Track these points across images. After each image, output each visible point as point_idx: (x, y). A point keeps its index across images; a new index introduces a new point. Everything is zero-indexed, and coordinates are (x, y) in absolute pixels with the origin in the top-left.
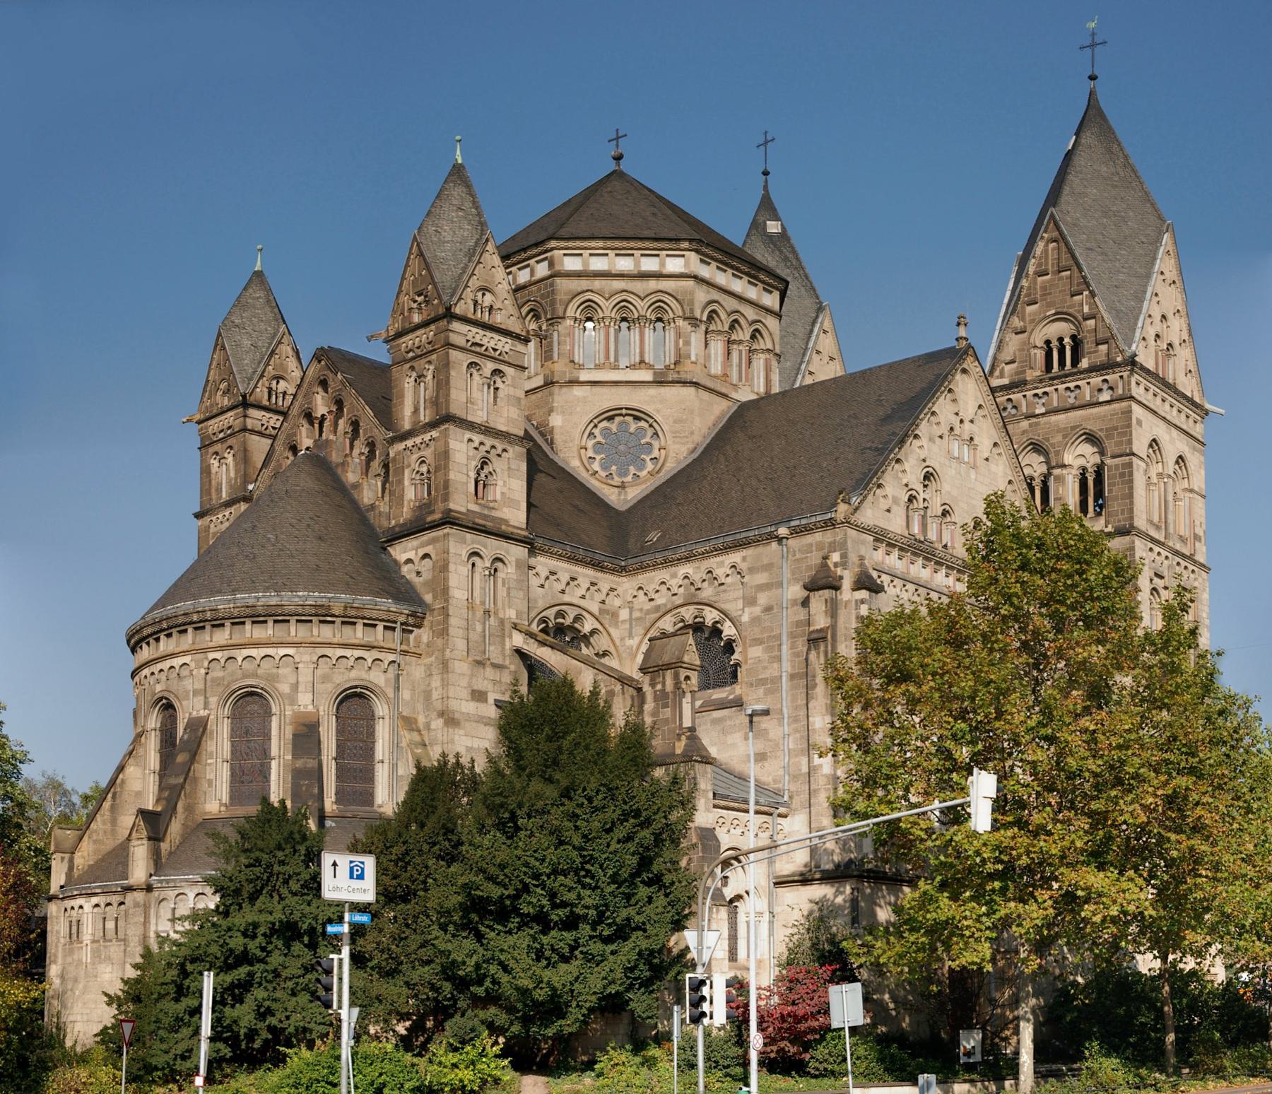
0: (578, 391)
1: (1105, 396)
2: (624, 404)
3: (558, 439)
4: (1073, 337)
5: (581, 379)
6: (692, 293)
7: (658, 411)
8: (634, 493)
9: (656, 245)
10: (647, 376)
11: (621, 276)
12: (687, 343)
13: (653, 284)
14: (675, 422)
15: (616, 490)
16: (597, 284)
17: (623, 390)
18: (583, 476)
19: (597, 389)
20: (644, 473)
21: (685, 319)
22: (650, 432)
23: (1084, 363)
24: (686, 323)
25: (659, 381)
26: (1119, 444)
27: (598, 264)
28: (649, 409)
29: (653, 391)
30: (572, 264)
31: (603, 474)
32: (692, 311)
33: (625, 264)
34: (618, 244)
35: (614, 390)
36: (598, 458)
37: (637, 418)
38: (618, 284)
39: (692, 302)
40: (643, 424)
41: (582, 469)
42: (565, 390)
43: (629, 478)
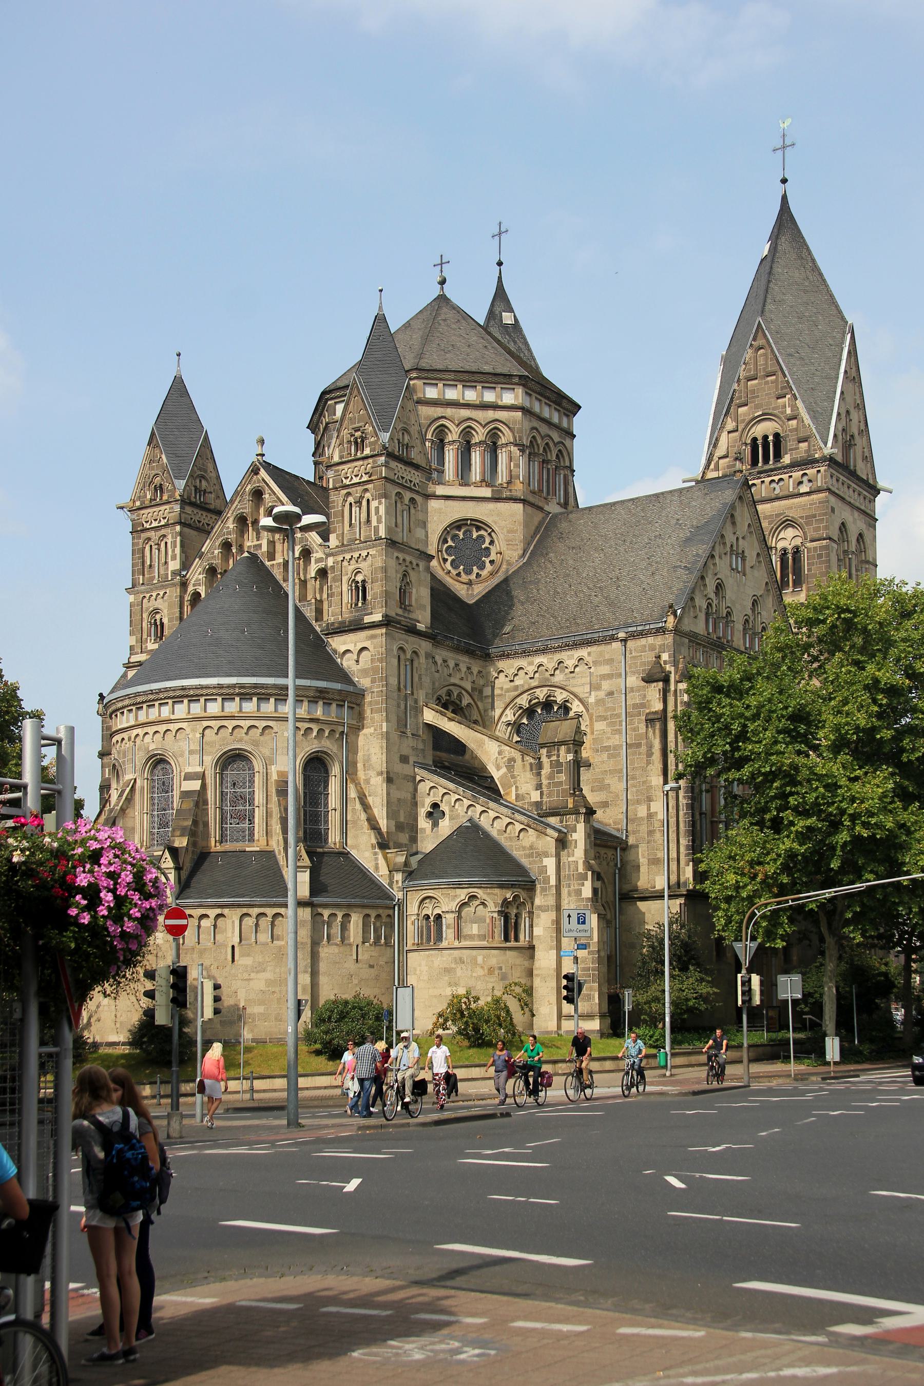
2: (470, 514)
4: (777, 436)
5: (437, 493)
7: (495, 523)
8: (479, 590)
10: (487, 492)
11: (467, 406)
12: (517, 466)
13: (491, 414)
14: (508, 532)
15: (465, 586)
16: (449, 412)
19: (450, 503)
20: (484, 573)
21: (516, 445)
22: (488, 540)
24: (516, 448)
25: (496, 499)
28: (489, 520)
29: (491, 506)
31: (454, 572)
35: (462, 503)
36: (450, 559)
37: (478, 528)
38: (465, 413)
40: (482, 532)
41: (439, 568)
43: (473, 577)
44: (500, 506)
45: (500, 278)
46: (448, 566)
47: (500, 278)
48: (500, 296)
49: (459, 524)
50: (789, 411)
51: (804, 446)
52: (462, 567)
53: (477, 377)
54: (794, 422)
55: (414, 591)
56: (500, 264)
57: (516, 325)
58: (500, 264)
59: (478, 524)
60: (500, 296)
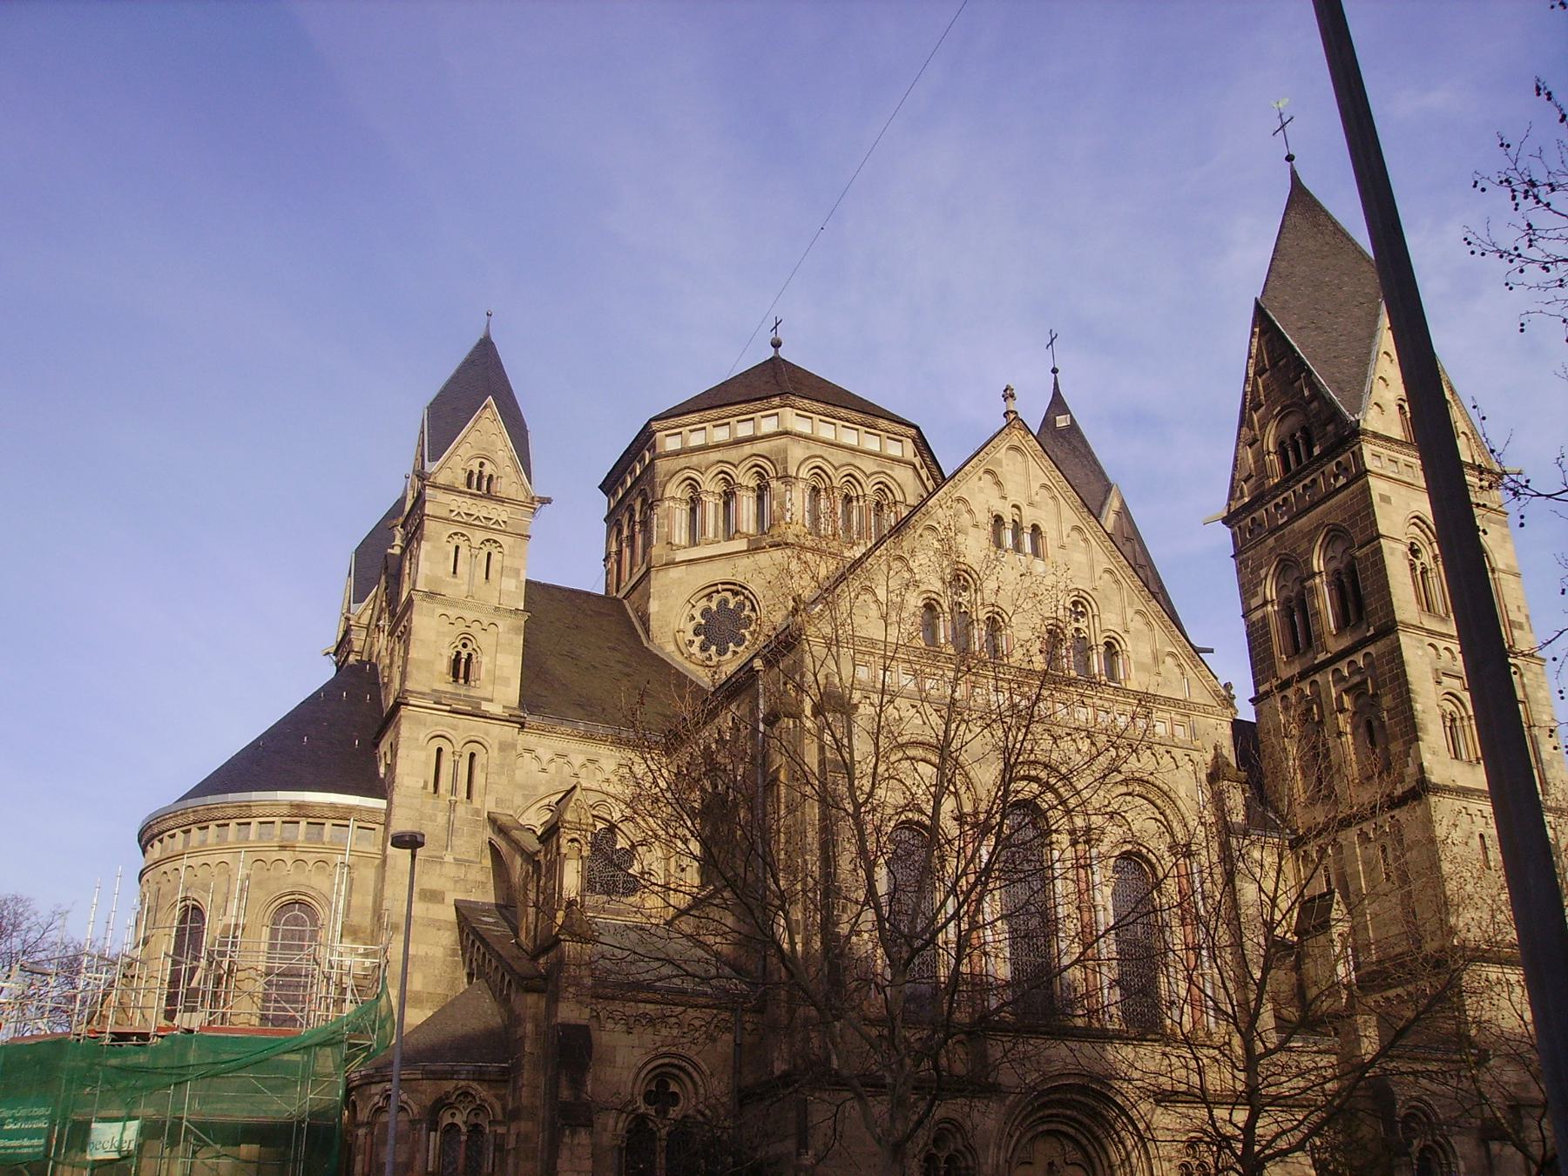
0: (674, 573)
1: (1342, 480)
3: (653, 624)
4: (1304, 430)
6: (785, 451)
9: (751, 406)
11: (717, 446)
13: (748, 449)
16: (695, 459)
17: (718, 564)
18: (678, 661)
21: (778, 479)
23: (1316, 451)
25: (754, 548)
27: (696, 439)
29: (745, 562)
30: (672, 444)
31: (701, 656)
32: (785, 469)
33: (721, 435)
34: (714, 413)
35: (708, 566)
36: (698, 640)
38: (714, 456)
39: (785, 461)
42: (661, 573)
44: (762, 558)
45: (1056, 384)
46: (695, 649)
47: (1056, 384)
48: (1058, 403)
49: (710, 591)
50: (1306, 393)
51: (1330, 428)
52: (714, 648)
53: (934, 469)
54: (1315, 404)
55: (485, 660)
56: (1055, 371)
57: (1073, 427)
59: (737, 589)
60: (1058, 403)
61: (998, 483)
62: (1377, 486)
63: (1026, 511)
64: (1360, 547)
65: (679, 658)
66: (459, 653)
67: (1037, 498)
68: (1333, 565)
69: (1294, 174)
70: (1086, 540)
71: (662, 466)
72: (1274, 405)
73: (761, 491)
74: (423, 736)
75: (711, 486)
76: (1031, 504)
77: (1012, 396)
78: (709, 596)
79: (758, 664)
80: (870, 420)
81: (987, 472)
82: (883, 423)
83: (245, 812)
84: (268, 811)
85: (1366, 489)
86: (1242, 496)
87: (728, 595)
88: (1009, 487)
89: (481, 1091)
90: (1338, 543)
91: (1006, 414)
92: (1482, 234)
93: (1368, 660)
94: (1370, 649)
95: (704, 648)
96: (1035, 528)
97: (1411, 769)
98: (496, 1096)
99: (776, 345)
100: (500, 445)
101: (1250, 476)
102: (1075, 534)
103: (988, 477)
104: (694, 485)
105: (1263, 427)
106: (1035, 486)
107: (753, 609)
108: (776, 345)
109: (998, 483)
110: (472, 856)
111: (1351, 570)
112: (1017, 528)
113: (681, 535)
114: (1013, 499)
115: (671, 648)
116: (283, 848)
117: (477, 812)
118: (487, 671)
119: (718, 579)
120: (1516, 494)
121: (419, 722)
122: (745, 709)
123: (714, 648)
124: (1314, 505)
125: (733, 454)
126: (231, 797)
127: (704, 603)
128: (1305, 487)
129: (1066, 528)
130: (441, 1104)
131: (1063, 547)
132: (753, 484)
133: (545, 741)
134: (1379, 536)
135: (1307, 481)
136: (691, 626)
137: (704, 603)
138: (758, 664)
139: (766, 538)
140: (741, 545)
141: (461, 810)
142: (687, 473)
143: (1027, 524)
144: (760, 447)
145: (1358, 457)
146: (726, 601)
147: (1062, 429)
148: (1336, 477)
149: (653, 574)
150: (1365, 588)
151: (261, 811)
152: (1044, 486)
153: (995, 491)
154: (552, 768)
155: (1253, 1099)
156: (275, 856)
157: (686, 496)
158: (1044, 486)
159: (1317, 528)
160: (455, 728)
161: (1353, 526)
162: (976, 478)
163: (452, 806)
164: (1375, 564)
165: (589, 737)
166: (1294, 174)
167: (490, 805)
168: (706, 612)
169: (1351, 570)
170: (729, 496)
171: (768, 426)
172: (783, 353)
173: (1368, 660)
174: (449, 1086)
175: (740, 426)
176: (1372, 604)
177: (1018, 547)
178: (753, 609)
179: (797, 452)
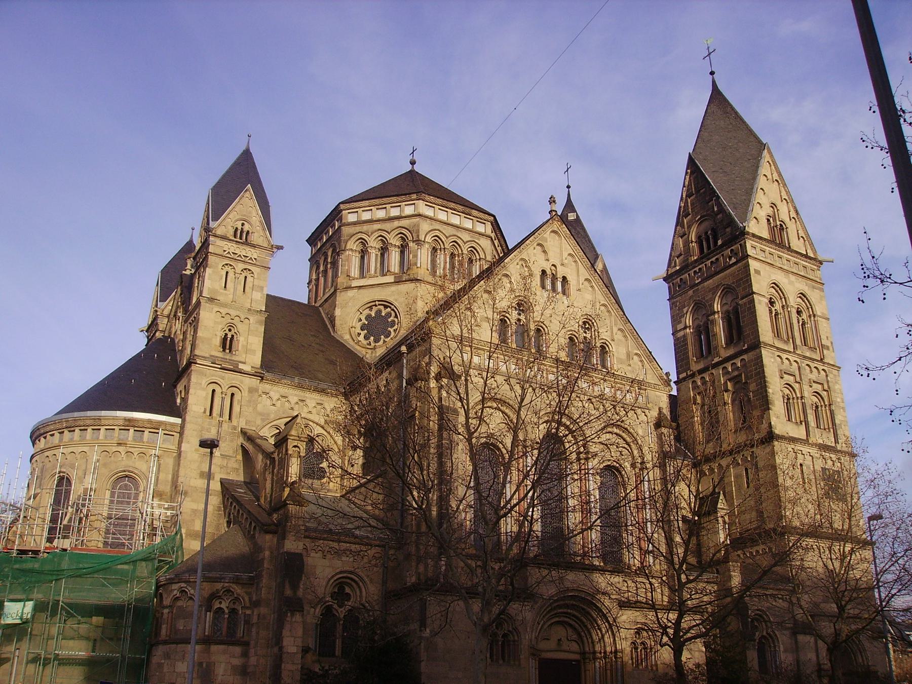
0: (350, 293)
1: (733, 260)
3: (338, 322)
4: (713, 230)
6: (418, 226)
11: (378, 221)
12: (415, 256)
13: (396, 223)
16: (365, 228)
18: (351, 344)
19: (361, 291)
22: (393, 314)
23: (720, 242)
25: (398, 282)
26: (744, 289)
27: (366, 216)
29: (394, 288)
30: (352, 218)
31: (365, 342)
32: (418, 236)
33: (381, 214)
34: (377, 201)
35: (371, 290)
36: (363, 333)
38: (377, 226)
39: (418, 231)
40: (389, 309)
46: (361, 338)
48: (569, 206)
51: (728, 230)
52: (372, 338)
54: (720, 216)
55: (241, 339)
56: (568, 187)
58: (568, 187)
59: (387, 304)
60: (569, 206)
61: (545, 252)
62: (753, 265)
63: (559, 268)
64: (742, 298)
65: (352, 343)
66: (226, 334)
67: (566, 261)
68: (726, 308)
69: (714, 83)
70: (592, 287)
71: (346, 230)
72: (697, 215)
73: (403, 248)
74: (204, 382)
75: (374, 244)
76: (562, 265)
77: (554, 202)
78: (371, 308)
79: (404, 349)
80: (468, 210)
81: (539, 245)
82: (475, 212)
83: (97, 422)
84: (111, 422)
85: (747, 266)
86: (675, 266)
87: (382, 307)
88: (551, 254)
89: (238, 590)
90: (730, 295)
91: (550, 212)
92: (871, 137)
93: (743, 362)
94: (745, 357)
95: (366, 338)
96: (564, 278)
97: (765, 425)
98: (246, 592)
99: (413, 163)
100: (254, 214)
101: (680, 255)
102: (586, 283)
103: (539, 248)
104: (364, 243)
105: (689, 227)
106: (565, 255)
107: (396, 316)
108: (413, 163)
109: (545, 252)
110: (231, 453)
111: (736, 311)
112: (554, 278)
113: (355, 272)
114: (552, 261)
115: (347, 337)
116: (119, 444)
117: (235, 428)
118: (243, 346)
119: (376, 298)
120: (882, 281)
121: (203, 374)
122: (394, 374)
123: (372, 338)
124: (717, 273)
125: (388, 226)
126: (89, 413)
127: (367, 312)
128: (712, 262)
129: (582, 280)
130: (214, 596)
131: (579, 290)
132: (398, 243)
133: (275, 388)
134: (753, 293)
135: (713, 259)
136: (359, 325)
137: (367, 312)
138: (404, 349)
139: (406, 276)
140: (391, 279)
141: (225, 426)
142: (360, 235)
143: (560, 275)
144: (404, 223)
145: (744, 247)
146: (380, 311)
147: (571, 221)
148: (730, 258)
149: (338, 294)
150: (743, 322)
151: (107, 422)
152: (570, 255)
153: (542, 255)
154: (278, 404)
155: (682, 609)
156: (115, 449)
157: (359, 249)
158: (570, 255)
159: (717, 286)
160: (223, 378)
161: (739, 286)
162: (532, 248)
163: (220, 424)
164: (749, 308)
165: (300, 387)
166: (714, 83)
167: (243, 424)
168: (368, 317)
169: (736, 311)
170: (384, 250)
171: (409, 210)
172: (417, 168)
173: (743, 362)
174: (219, 586)
175: (392, 210)
176: (747, 331)
177: (554, 289)
178: (396, 316)
179: (425, 226)
